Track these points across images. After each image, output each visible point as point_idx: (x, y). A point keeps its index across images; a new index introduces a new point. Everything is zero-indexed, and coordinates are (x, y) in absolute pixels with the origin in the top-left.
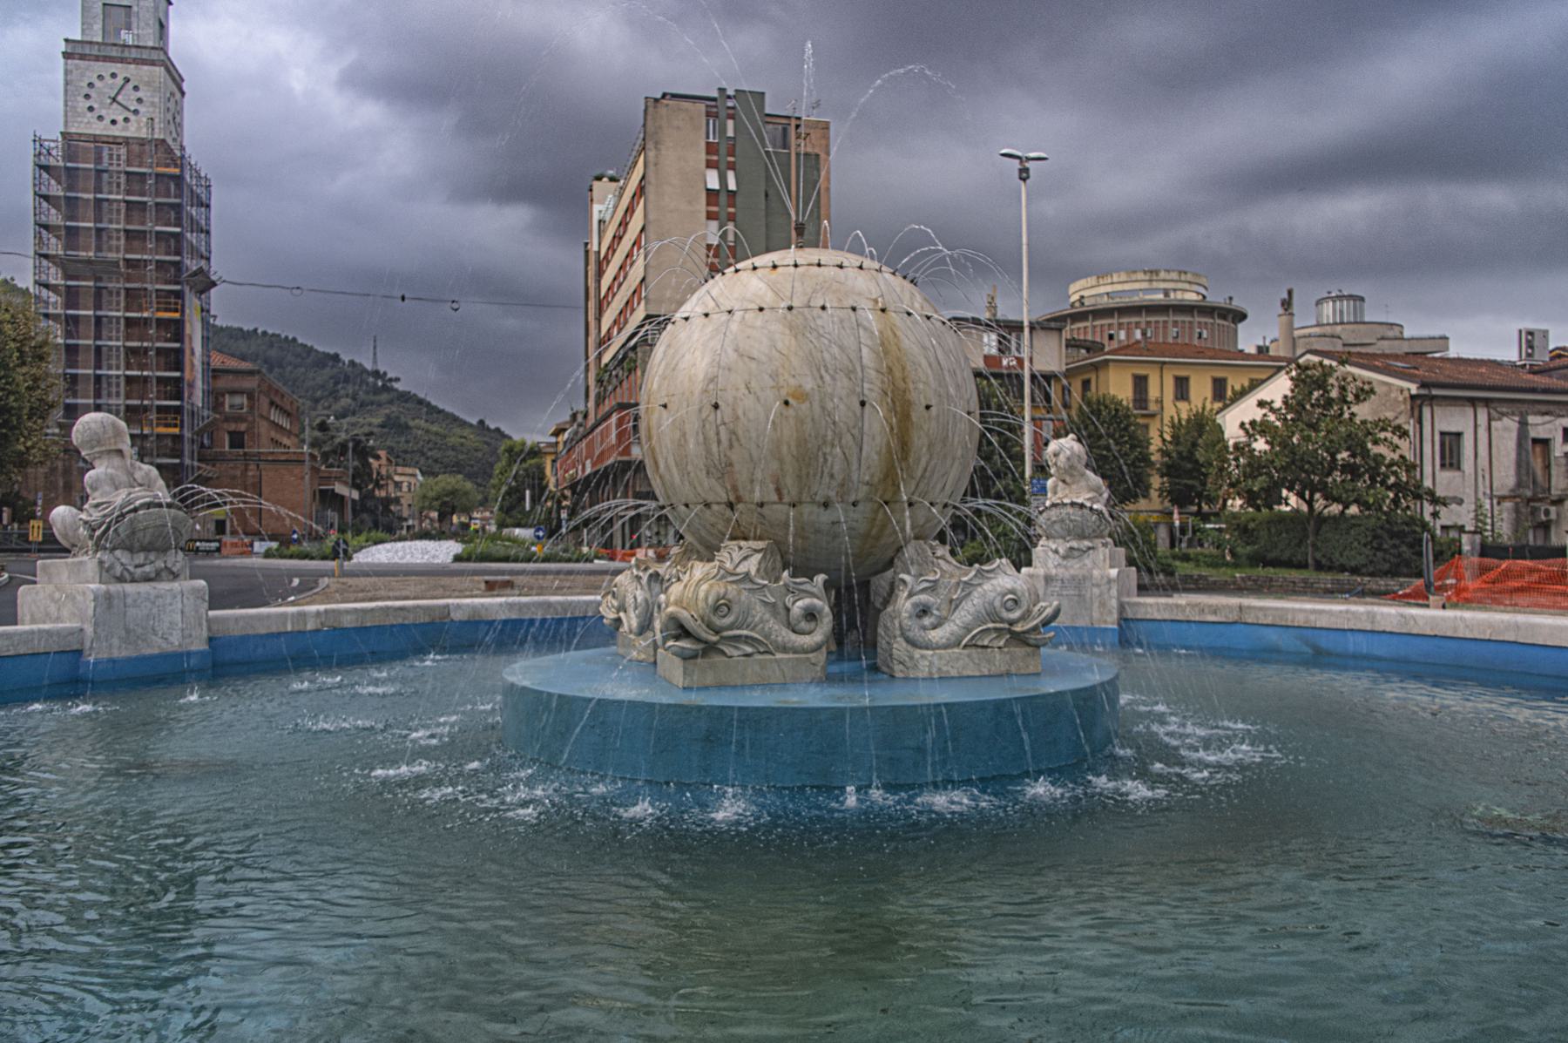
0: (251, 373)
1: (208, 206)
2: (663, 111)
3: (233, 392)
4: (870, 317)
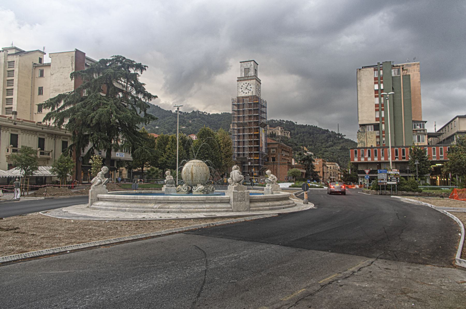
0: (276, 144)
1: (266, 107)
2: (362, 72)
3: (273, 148)
4: (191, 167)
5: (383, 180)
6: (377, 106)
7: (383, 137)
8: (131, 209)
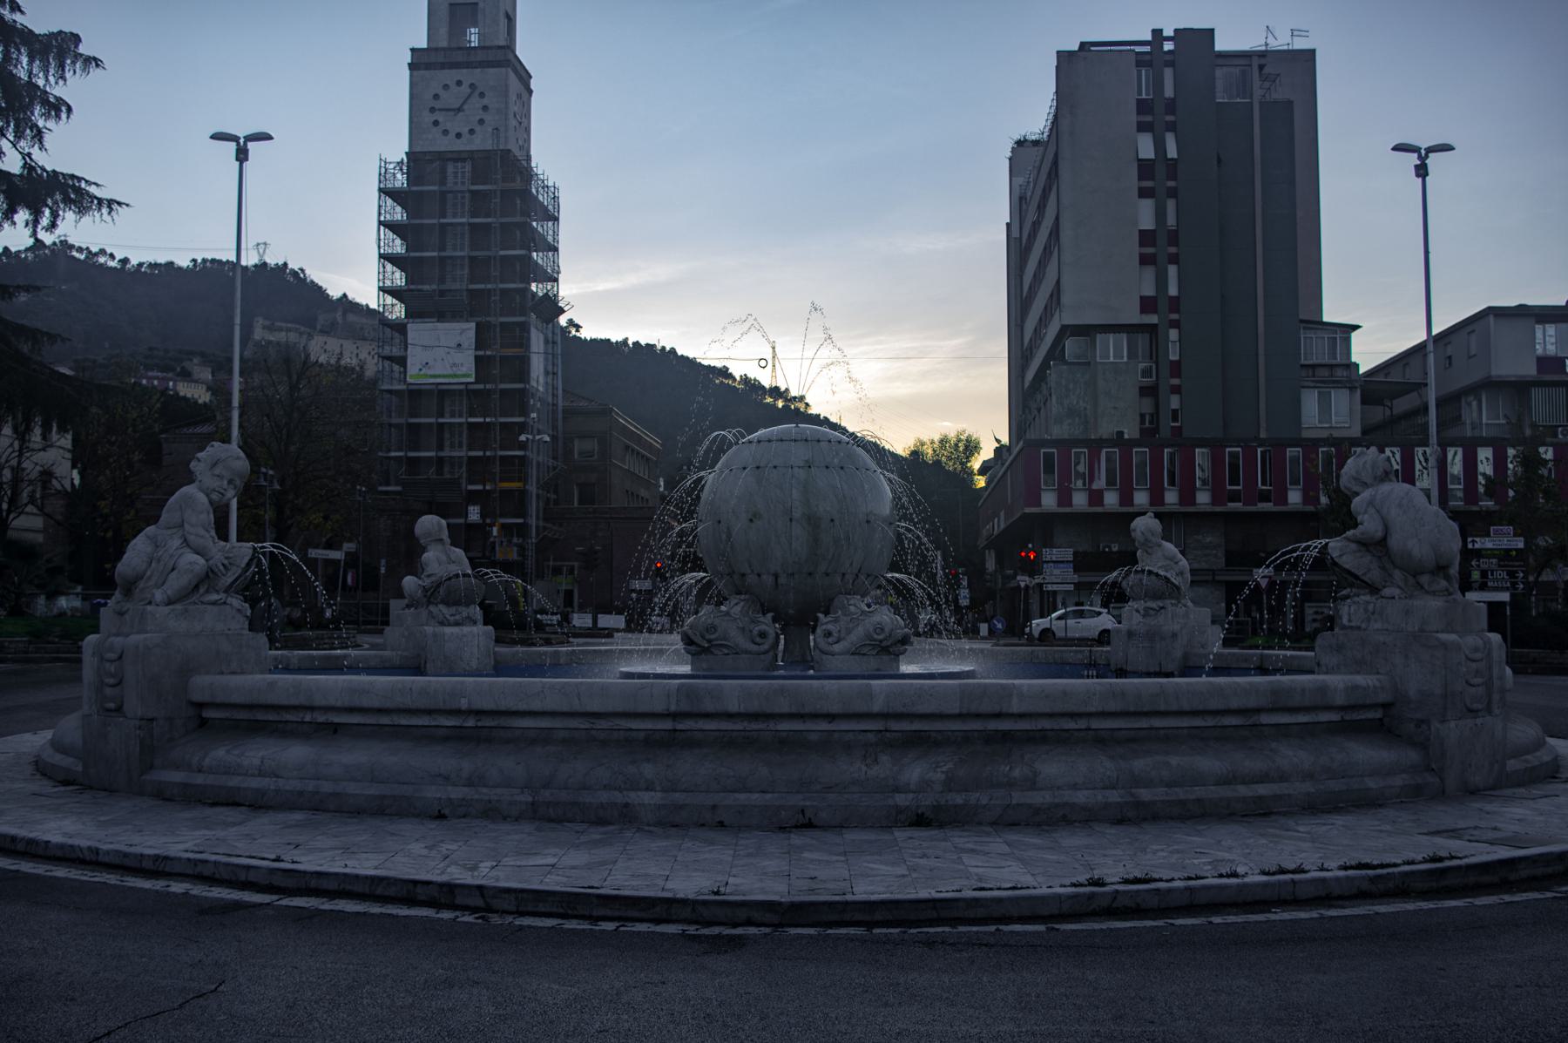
6: (1146, 238)
7: (1176, 390)
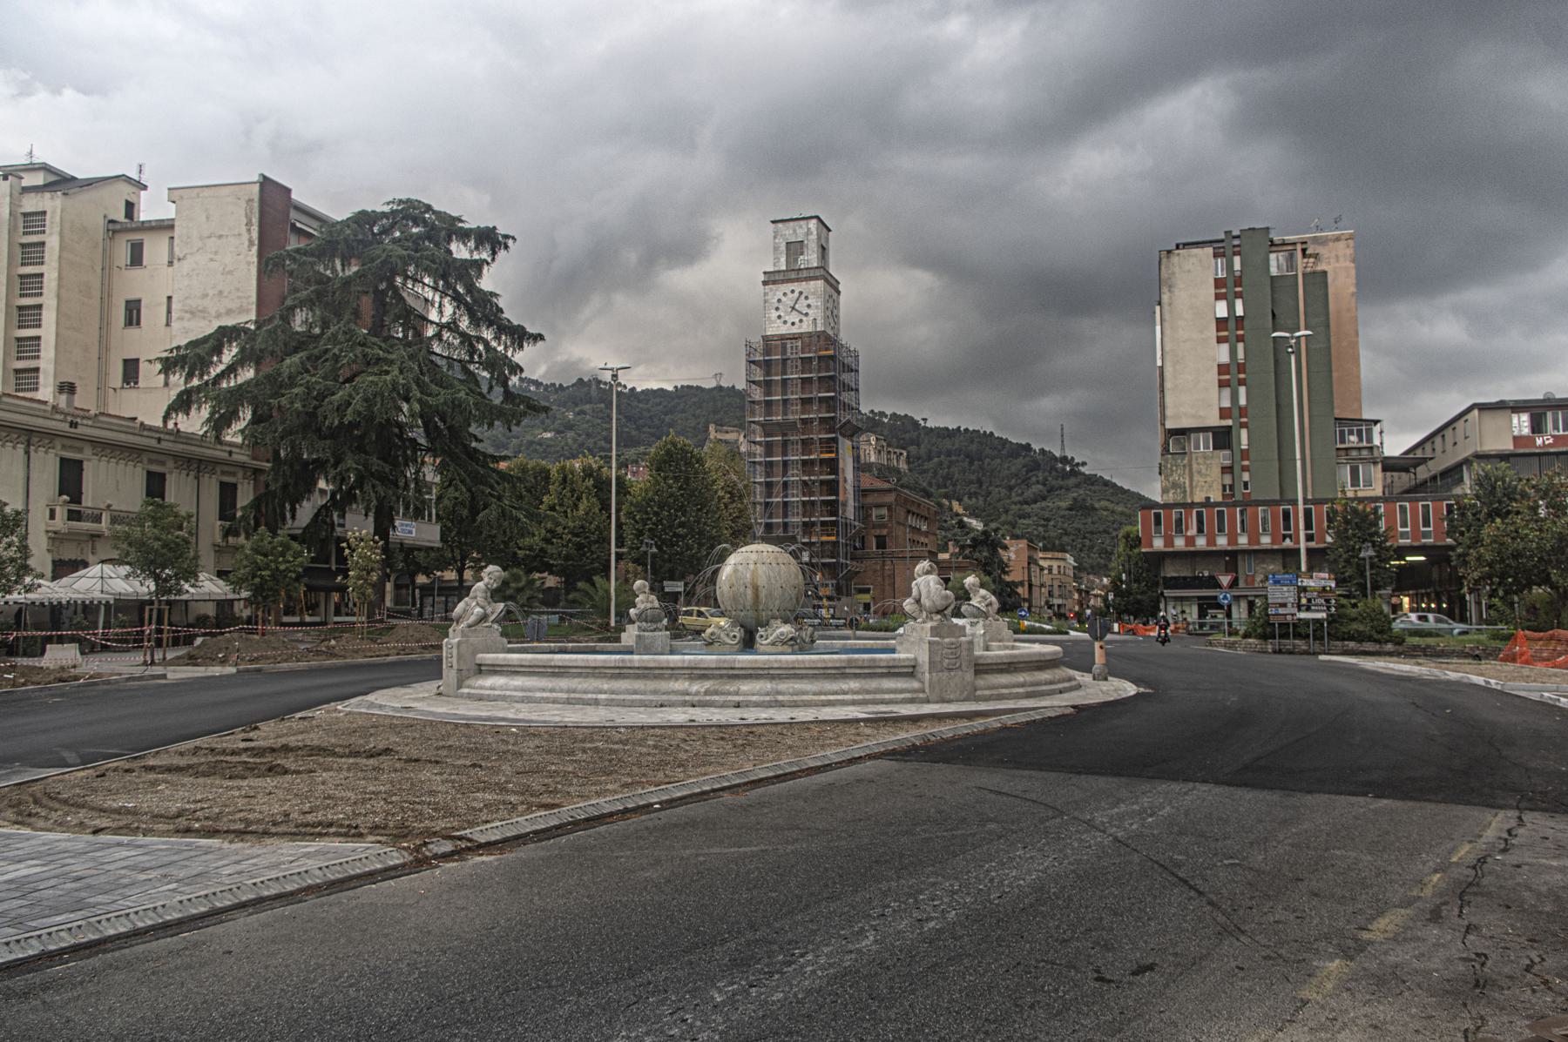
0: (889, 491)
1: (857, 371)
2: (1175, 259)
3: (879, 506)
4: (752, 566)
5: (1284, 605)
6: (1222, 369)
7: (1245, 469)
8: (613, 696)
